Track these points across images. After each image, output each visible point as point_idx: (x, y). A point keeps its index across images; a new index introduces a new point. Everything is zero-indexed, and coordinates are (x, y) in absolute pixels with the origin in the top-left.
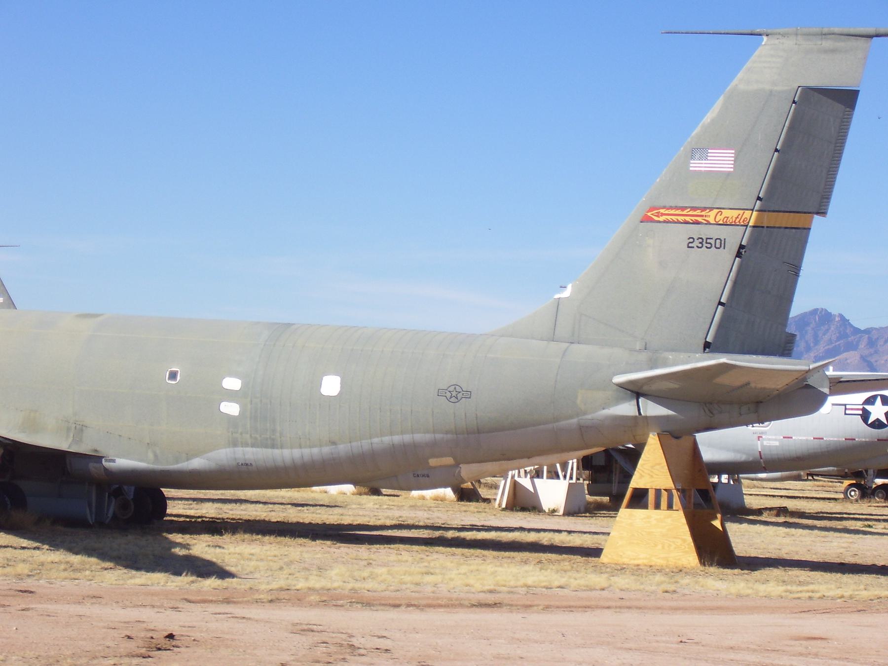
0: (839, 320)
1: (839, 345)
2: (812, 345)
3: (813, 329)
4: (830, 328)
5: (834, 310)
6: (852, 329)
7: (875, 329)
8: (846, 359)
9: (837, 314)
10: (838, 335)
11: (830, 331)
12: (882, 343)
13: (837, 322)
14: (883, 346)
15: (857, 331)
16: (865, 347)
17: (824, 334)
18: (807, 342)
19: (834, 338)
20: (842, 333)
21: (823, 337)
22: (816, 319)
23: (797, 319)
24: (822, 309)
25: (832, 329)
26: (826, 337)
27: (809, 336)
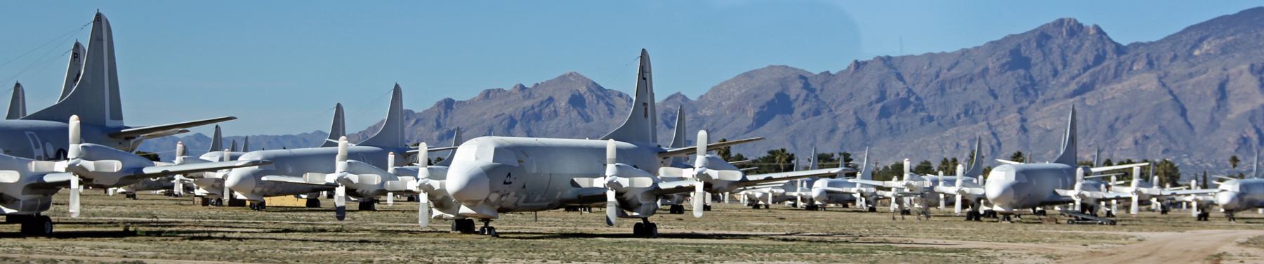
0: (1094, 34)
1: (1108, 66)
2: (1060, 67)
3: (1059, 46)
4: (1082, 44)
5: (1087, 21)
6: (1114, 46)
7: (1143, 44)
8: (1139, 85)
9: (1091, 25)
10: (1096, 53)
11: (1084, 48)
12: (1167, 63)
13: (1092, 36)
14: (1169, 66)
15: (1120, 50)
16: (1143, 67)
17: (1075, 53)
18: (1052, 64)
19: (1091, 59)
20: (1101, 51)
21: (1075, 56)
22: (1062, 33)
23: (1037, 33)
24: (1070, 19)
25: (1086, 45)
26: (1079, 57)
27: (1056, 57)
